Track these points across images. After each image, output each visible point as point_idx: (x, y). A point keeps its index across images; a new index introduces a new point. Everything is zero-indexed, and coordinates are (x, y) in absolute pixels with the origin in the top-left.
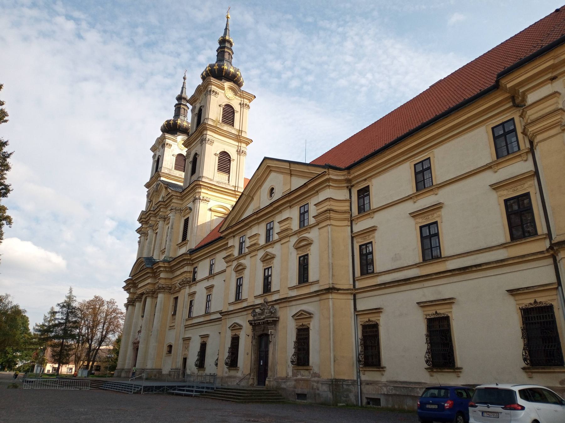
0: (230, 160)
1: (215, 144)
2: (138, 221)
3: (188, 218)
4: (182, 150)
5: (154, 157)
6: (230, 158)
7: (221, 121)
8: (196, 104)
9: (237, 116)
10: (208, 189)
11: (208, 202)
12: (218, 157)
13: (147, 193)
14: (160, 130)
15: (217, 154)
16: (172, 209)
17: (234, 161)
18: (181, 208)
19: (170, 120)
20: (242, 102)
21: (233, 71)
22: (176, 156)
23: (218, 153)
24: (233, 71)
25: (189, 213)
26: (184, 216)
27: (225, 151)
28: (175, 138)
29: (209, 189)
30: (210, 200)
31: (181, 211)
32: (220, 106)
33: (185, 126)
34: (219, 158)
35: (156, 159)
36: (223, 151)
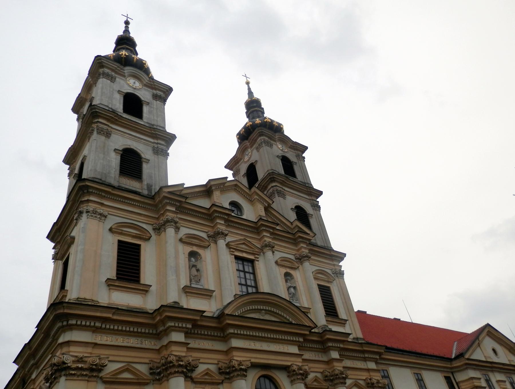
9: (296, 168)
21: (277, 125)
24: (277, 125)
27: (300, 205)
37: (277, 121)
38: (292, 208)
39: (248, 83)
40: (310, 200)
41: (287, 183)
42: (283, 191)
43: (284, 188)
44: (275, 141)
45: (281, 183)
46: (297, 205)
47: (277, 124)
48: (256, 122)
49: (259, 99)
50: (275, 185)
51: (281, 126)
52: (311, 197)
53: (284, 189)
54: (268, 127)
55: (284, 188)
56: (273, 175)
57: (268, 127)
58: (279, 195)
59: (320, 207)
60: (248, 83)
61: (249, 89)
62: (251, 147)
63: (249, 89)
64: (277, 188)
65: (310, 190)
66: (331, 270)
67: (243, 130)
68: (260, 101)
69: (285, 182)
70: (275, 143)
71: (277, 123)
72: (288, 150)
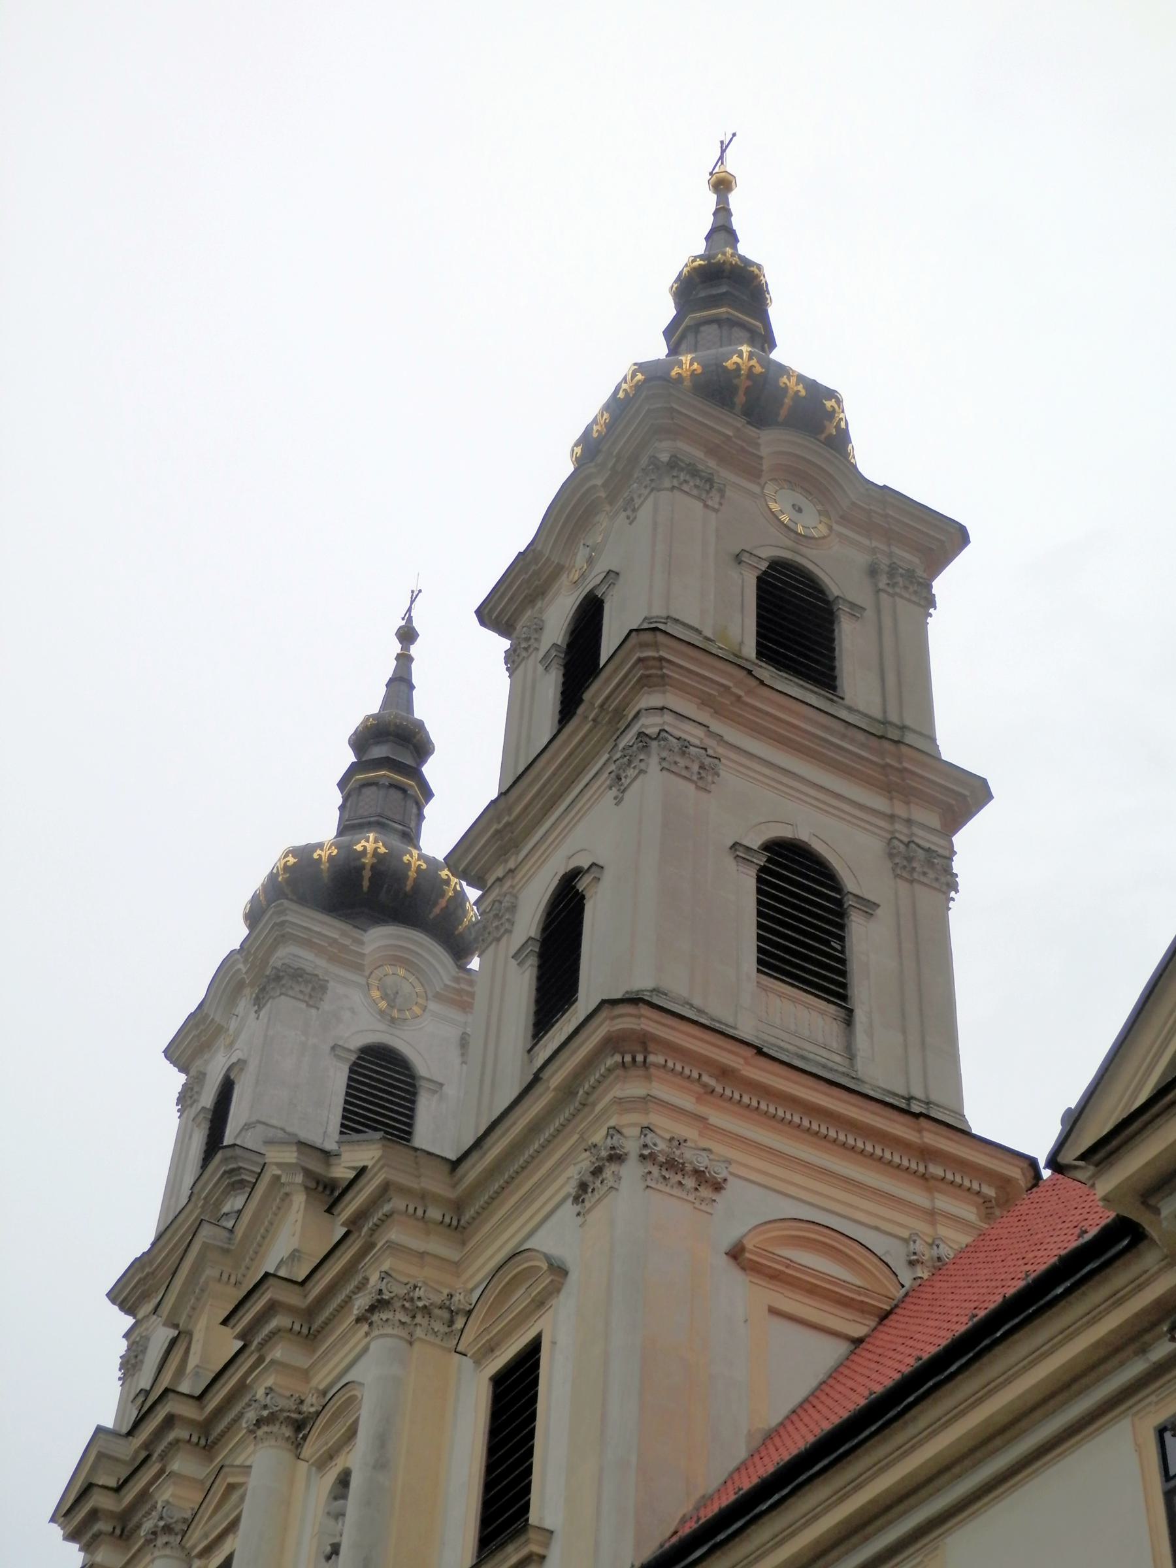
0: (839, 903)
1: (730, 778)
2: (55, 1526)
3: (533, 1350)
4: (393, 1021)
5: (185, 1098)
6: (837, 887)
7: (750, 650)
8: (541, 611)
10: (706, 1078)
11: (705, 1192)
12: (753, 873)
13: (122, 1346)
14: (242, 921)
15: (748, 849)
16: (380, 1304)
17: (879, 912)
18: (451, 1296)
19: (320, 846)
20: (885, 561)
21: (803, 393)
22: (353, 1057)
23: (755, 844)
24: (803, 393)
25: (540, 1303)
26: (491, 1349)
28: (347, 942)
29: (712, 1082)
30: (730, 1179)
31: (451, 1323)
32: (738, 559)
33: (412, 874)
34: (759, 880)
35: (208, 1098)
36: (790, 836)
37: (811, 375)
38: (736, 844)
39: (722, 185)
40: (892, 818)
41: (746, 704)
42: (710, 742)
43: (716, 726)
44: (753, 472)
45: (706, 702)
46: (786, 833)
47: (800, 387)
48: (673, 373)
49: (752, 263)
50: (659, 704)
51: (829, 404)
52: (908, 803)
53: (720, 738)
54: (740, 399)
55: (716, 726)
56: (656, 646)
57: (740, 399)
58: (665, 764)
59: (948, 871)
60: (722, 185)
61: (723, 212)
62: (611, 503)
63: (723, 212)
64: (668, 718)
65: (900, 759)
66: (906, 1241)
67: (606, 415)
68: (756, 277)
69: (739, 698)
70: (756, 489)
71: (801, 378)
72: (830, 528)
